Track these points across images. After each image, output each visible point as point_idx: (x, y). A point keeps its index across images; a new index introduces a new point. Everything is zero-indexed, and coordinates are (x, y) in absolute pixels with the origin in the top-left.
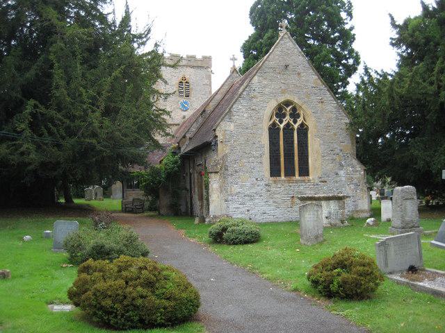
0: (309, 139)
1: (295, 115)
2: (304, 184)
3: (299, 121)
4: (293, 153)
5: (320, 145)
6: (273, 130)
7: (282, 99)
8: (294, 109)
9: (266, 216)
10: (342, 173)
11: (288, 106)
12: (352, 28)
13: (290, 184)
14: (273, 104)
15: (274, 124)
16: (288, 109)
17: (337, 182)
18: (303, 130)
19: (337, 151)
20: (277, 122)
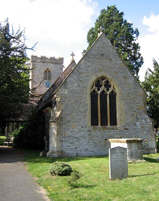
0: (117, 101)
1: (108, 85)
2: (114, 131)
3: (110, 90)
4: (107, 110)
5: (124, 105)
6: (93, 95)
7: (99, 75)
8: (107, 82)
9: (88, 152)
10: (138, 123)
11: (103, 79)
12: (132, 28)
13: (104, 131)
14: (94, 78)
15: (94, 91)
16: (103, 82)
17: (135, 129)
18: (113, 96)
19: (135, 109)
20: (96, 90)
